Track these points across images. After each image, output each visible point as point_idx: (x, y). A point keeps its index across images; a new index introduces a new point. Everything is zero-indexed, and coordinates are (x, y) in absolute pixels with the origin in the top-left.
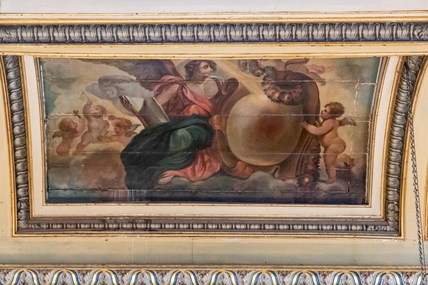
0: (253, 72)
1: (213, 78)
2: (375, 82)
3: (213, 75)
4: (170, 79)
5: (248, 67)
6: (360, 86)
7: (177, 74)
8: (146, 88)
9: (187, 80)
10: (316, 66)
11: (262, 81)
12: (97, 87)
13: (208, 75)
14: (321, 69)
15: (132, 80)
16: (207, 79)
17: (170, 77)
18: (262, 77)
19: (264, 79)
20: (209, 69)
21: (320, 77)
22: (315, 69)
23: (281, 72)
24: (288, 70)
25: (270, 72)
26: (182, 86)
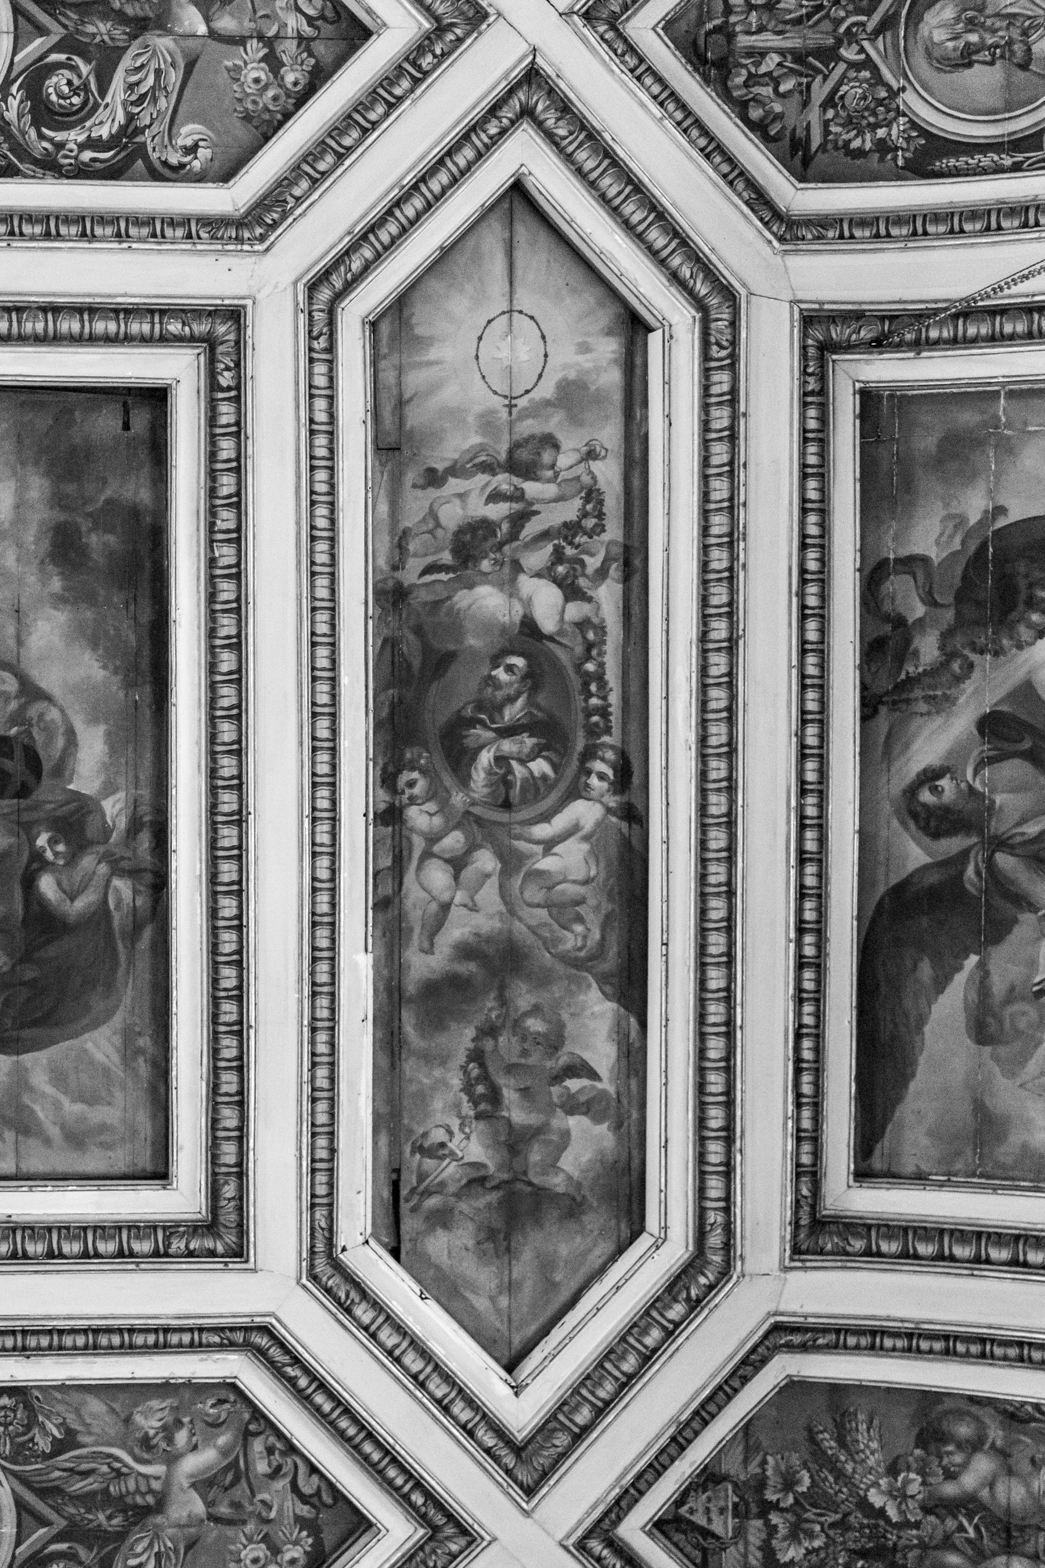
0: (959, 680)
1: (976, 773)
2: (998, 392)
3: (964, 771)
4: (978, 873)
5: (939, 693)
6: (1009, 425)
7: (964, 856)
8: (1009, 931)
9: (981, 832)
10: (941, 534)
11: (988, 657)
12: (1003, 1051)
13: (963, 785)
14: (951, 525)
15: (982, 965)
16: (978, 786)
17: (970, 872)
18: (974, 657)
19: (982, 652)
20: (945, 783)
21: (980, 522)
22: (951, 537)
23: (958, 614)
24: (950, 599)
25: (958, 641)
26: (1001, 843)
